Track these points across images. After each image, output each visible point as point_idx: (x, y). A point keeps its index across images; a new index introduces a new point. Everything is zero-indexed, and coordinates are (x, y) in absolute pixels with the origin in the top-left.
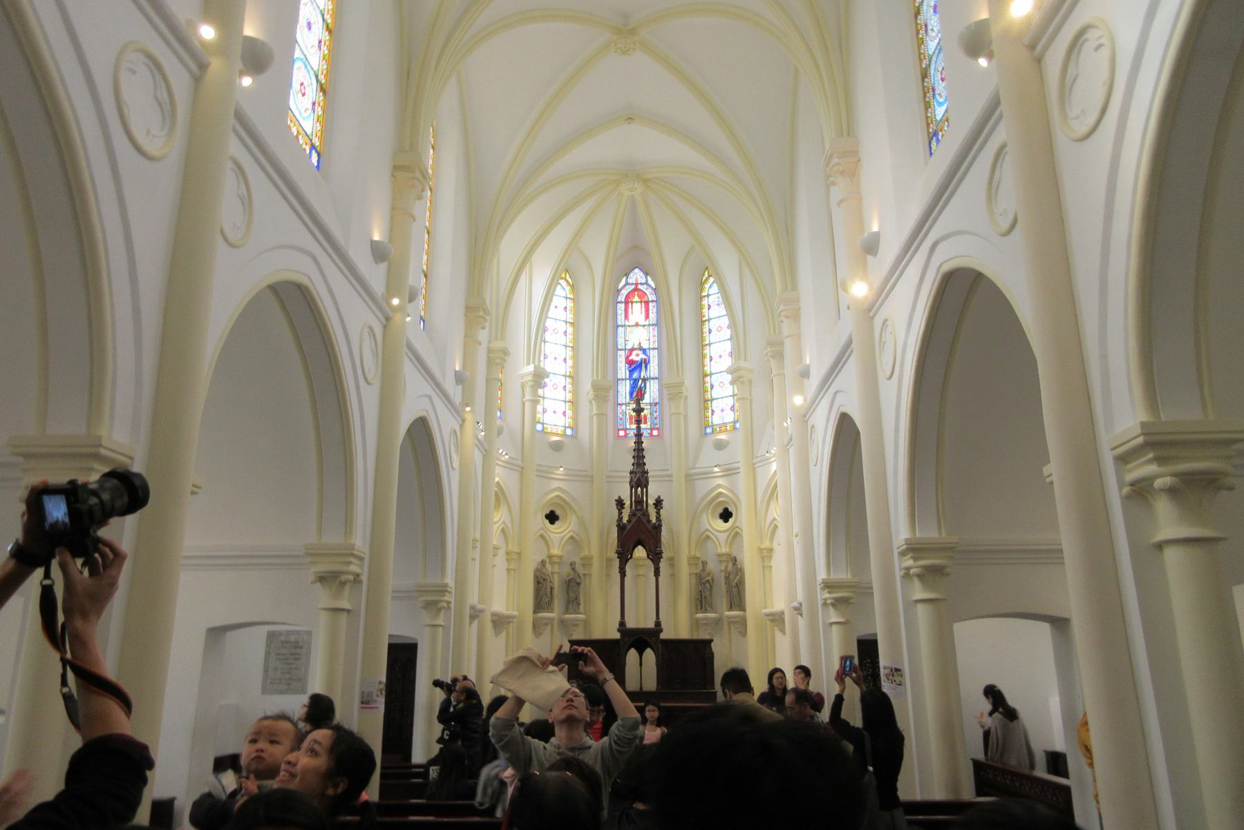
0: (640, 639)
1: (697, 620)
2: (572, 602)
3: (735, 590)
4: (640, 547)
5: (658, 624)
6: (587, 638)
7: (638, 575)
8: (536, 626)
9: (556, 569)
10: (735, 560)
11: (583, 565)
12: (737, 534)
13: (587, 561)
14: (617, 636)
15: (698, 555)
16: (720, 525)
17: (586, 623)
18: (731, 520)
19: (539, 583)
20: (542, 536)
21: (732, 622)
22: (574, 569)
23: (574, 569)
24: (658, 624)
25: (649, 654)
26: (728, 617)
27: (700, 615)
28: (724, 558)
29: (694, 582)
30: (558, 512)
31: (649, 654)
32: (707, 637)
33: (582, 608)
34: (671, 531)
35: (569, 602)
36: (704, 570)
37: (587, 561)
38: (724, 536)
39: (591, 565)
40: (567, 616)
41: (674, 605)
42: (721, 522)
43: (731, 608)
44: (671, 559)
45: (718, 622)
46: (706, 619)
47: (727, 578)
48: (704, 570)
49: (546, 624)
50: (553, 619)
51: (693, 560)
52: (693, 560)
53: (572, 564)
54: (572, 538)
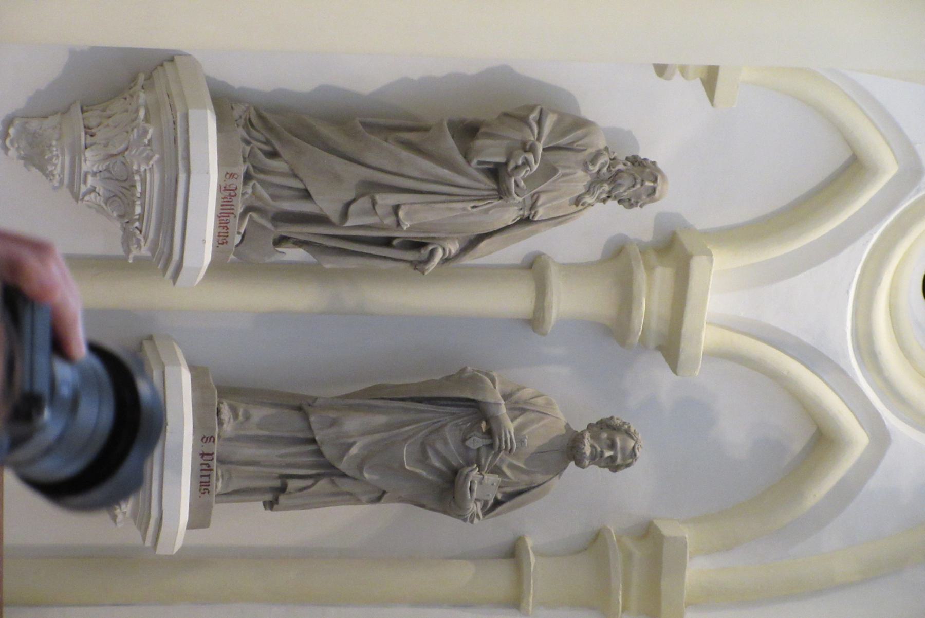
8: (116, 97)
9: (569, 301)
11: (595, 543)
19: (468, 132)
20: (853, 169)
22: (570, 450)
23: (570, 450)
33: (248, 524)
35: (301, 407)
49: (121, 193)
50: (166, 260)
53: (605, 444)
54: (823, 440)
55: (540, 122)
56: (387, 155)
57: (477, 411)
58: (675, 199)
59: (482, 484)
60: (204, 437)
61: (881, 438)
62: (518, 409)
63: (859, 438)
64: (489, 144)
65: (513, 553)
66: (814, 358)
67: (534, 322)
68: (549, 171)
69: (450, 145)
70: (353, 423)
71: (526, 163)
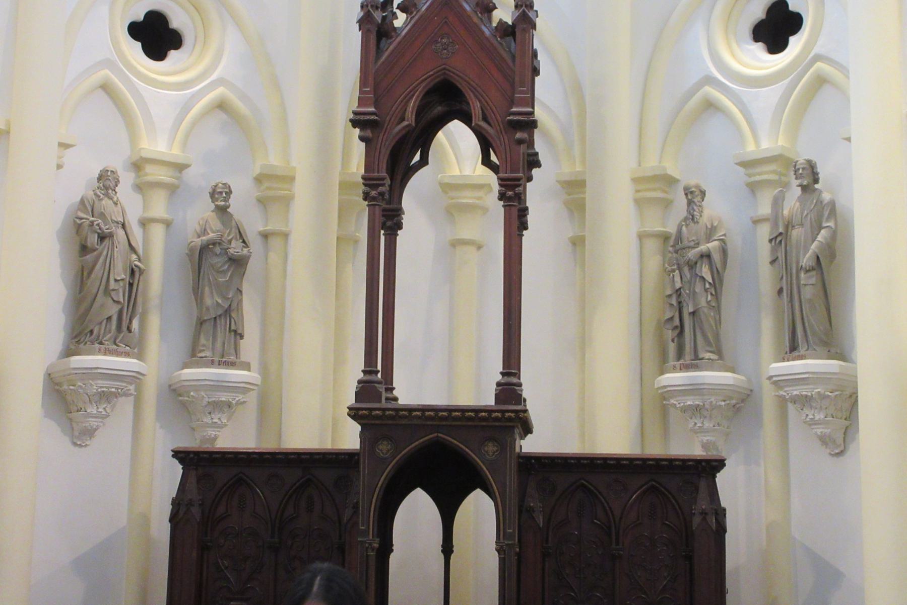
0: (442, 453)
1: (665, 395)
2: (215, 327)
3: (808, 283)
4: (456, 127)
5: (509, 391)
6: (269, 445)
7: (456, 243)
8: (65, 399)
9: (159, 207)
10: (810, 176)
11: (263, 202)
12: (821, 81)
13: (273, 188)
14: (350, 437)
15: (672, 169)
16: (757, 60)
17: (269, 405)
18: (796, 43)
19: (84, 249)
20: (106, 87)
21: (794, 398)
22: (222, 211)
23: (222, 211)
24: (509, 391)
25: (479, 511)
26: (778, 383)
27: (674, 378)
28: (766, 173)
29: (654, 263)
30: (177, 21)
31: (479, 511)
32: (696, 451)
33: (250, 347)
34: (576, 90)
35: (201, 323)
36: (691, 218)
37: (273, 188)
38: (770, 95)
39: (287, 201)
40: (191, 373)
41: (582, 343)
42: (759, 49)
43: (793, 349)
44: (574, 191)
45: (741, 404)
46: (695, 389)
47: (779, 240)
48: (691, 218)
49: (106, 397)
50: (136, 379)
51: (655, 187)
52: (655, 187)
53: (220, 195)
54: (222, 106)
55: (81, 219)
56: (94, 283)
57: (204, 250)
58: (117, 163)
59: (236, 248)
60: (212, 364)
61: (221, 81)
62: (205, 232)
63: (220, 90)
64: (90, 241)
65: (265, 236)
66: (186, 108)
67: (168, 224)
68: (102, 215)
69: (89, 257)
70: (208, 301)
71: (98, 225)
